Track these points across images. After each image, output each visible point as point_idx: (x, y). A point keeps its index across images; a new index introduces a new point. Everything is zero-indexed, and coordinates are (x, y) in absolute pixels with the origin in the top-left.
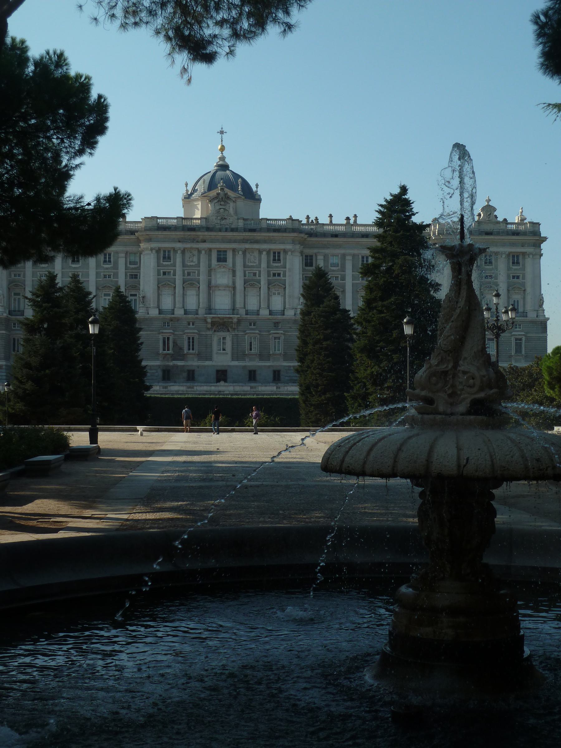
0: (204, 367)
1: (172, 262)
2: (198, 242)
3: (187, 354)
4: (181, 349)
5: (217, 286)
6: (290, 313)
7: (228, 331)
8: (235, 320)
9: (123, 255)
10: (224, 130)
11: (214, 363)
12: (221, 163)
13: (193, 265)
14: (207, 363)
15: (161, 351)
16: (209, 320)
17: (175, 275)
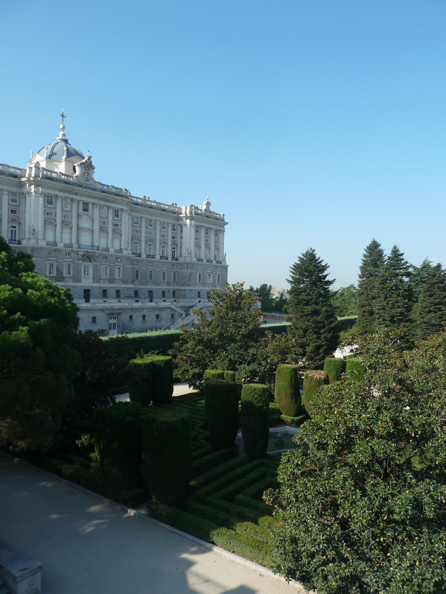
0: (76, 286)
1: (54, 206)
2: (72, 194)
3: (66, 277)
4: (61, 273)
5: (83, 229)
6: (125, 252)
7: (91, 261)
8: (97, 254)
9: (7, 193)
10: (65, 115)
11: (83, 285)
12: (64, 138)
13: (67, 211)
14: (79, 284)
15: (48, 275)
16: (82, 253)
17: (55, 216)
